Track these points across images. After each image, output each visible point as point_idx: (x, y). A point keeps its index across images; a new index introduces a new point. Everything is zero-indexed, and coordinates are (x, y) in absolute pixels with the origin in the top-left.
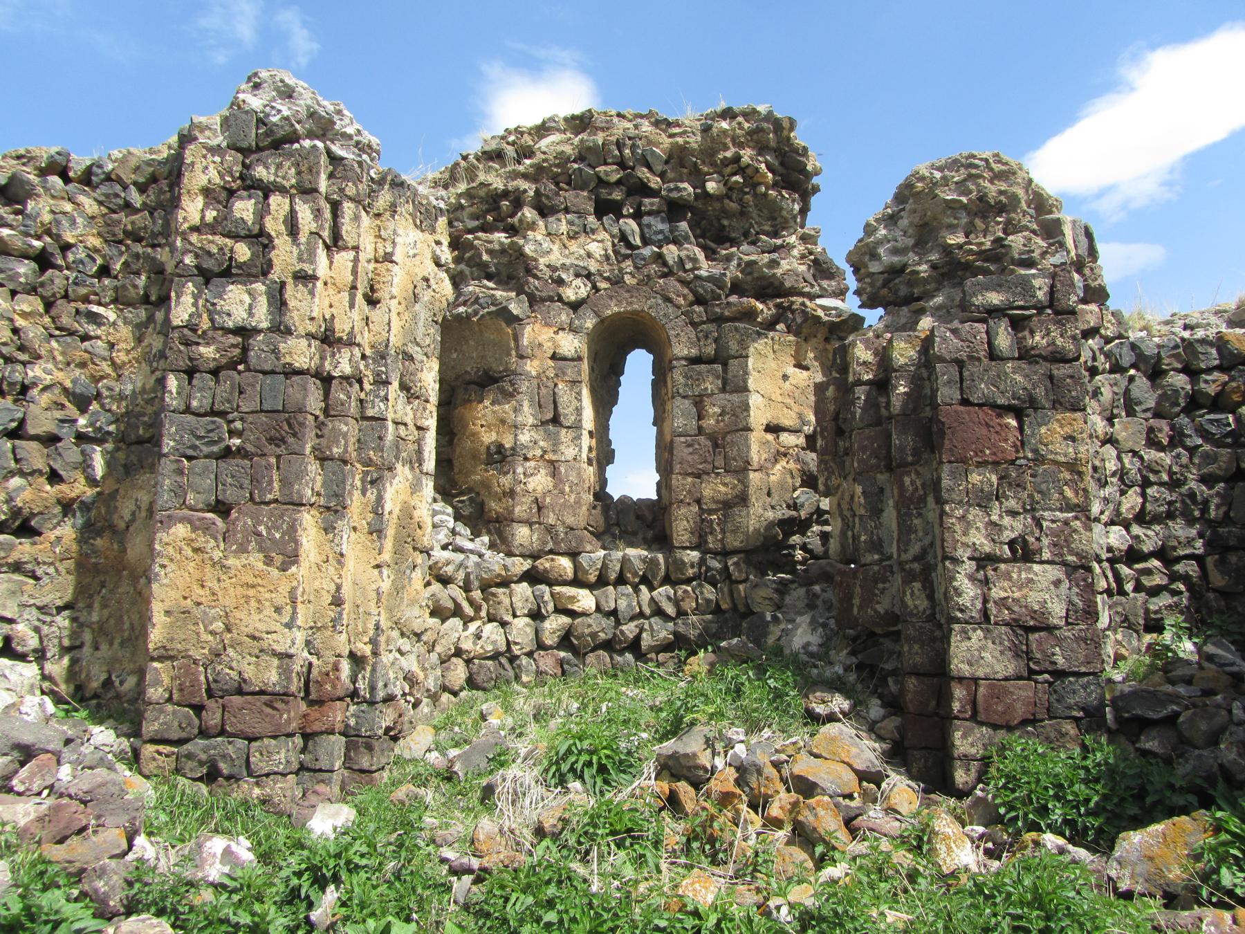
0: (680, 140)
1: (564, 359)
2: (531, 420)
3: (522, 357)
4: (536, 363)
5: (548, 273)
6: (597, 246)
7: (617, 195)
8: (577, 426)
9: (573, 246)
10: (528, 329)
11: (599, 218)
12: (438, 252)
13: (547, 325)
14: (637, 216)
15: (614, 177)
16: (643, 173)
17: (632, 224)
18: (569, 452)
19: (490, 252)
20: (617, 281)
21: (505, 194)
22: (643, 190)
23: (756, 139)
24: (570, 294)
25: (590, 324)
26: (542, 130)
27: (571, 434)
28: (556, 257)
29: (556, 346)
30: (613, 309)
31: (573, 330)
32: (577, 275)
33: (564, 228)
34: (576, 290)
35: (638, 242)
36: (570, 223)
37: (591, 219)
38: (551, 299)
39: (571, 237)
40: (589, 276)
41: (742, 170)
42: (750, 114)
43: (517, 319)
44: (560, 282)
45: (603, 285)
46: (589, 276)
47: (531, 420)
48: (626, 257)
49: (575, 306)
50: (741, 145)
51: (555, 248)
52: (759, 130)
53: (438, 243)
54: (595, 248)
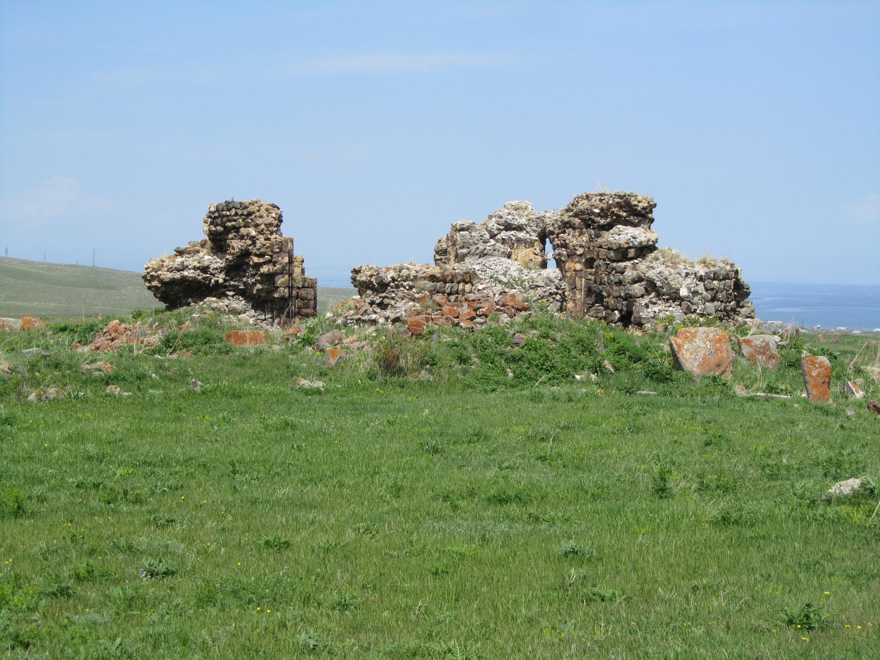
0: (603, 205)
1: (577, 271)
2: (568, 289)
3: (565, 272)
4: (570, 273)
5: (572, 247)
6: (585, 238)
7: (590, 223)
8: (581, 289)
9: (579, 239)
10: (567, 264)
11: (586, 229)
12: (535, 251)
13: (573, 262)
14: (593, 229)
15: (588, 218)
16: (593, 217)
17: (593, 232)
18: (578, 296)
19: (563, 240)
20: (589, 248)
21: (568, 222)
22: (593, 221)
23: (618, 205)
24: (578, 253)
25: (583, 261)
26: (582, 198)
27: (579, 292)
28: (575, 242)
29: (575, 268)
30: (588, 256)
31: (579, 262)
32: (580, 247)
33: (577, 234)
34: (580, 251)
35: (593, 236)
36: (578, 232)
37: (585, 230)
38: (573, 255)
39: (579, 236)
40: (583, 247)
41: (616, 215)
42: (620, 197)
43: (564, 262)
44: (576, 250)
45: (586, 249)
46: (583, 247)
47: (568, 289)
48: (591, 241)
49: (580, 255)
50: (615, 207)
51: (574, 240)
52: (618, 203)
53: (535, 249)
54: (584, 239)
